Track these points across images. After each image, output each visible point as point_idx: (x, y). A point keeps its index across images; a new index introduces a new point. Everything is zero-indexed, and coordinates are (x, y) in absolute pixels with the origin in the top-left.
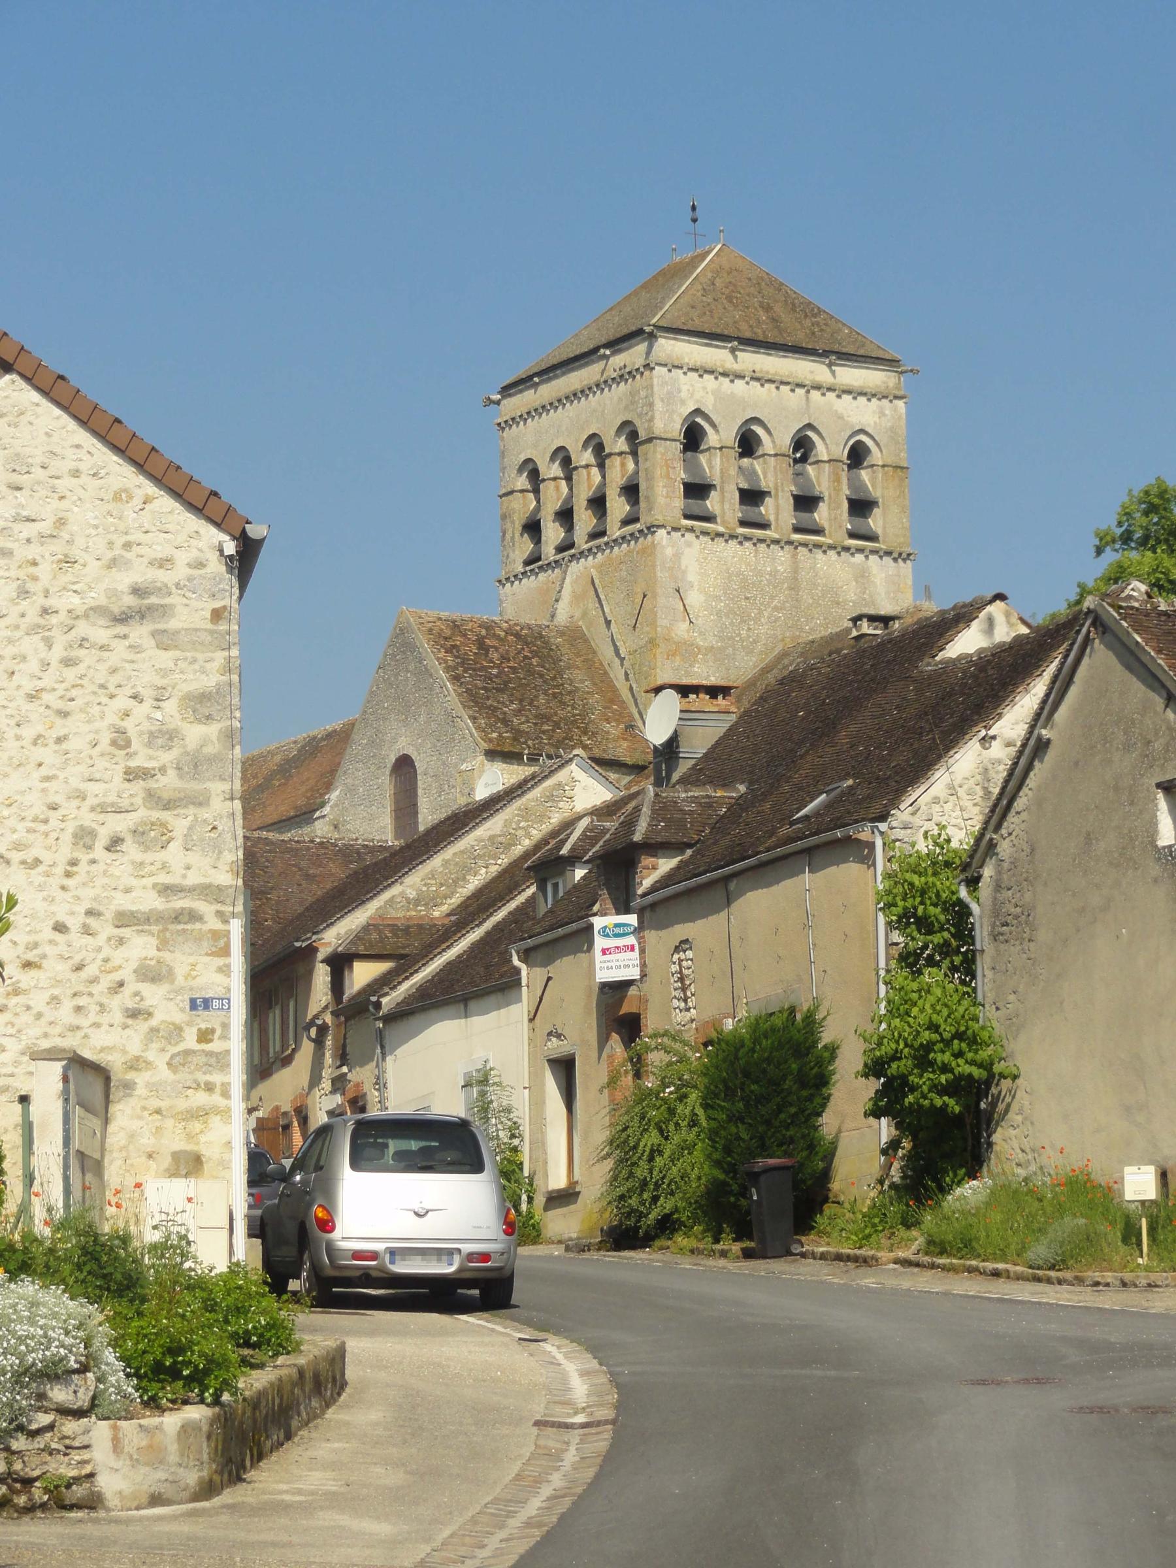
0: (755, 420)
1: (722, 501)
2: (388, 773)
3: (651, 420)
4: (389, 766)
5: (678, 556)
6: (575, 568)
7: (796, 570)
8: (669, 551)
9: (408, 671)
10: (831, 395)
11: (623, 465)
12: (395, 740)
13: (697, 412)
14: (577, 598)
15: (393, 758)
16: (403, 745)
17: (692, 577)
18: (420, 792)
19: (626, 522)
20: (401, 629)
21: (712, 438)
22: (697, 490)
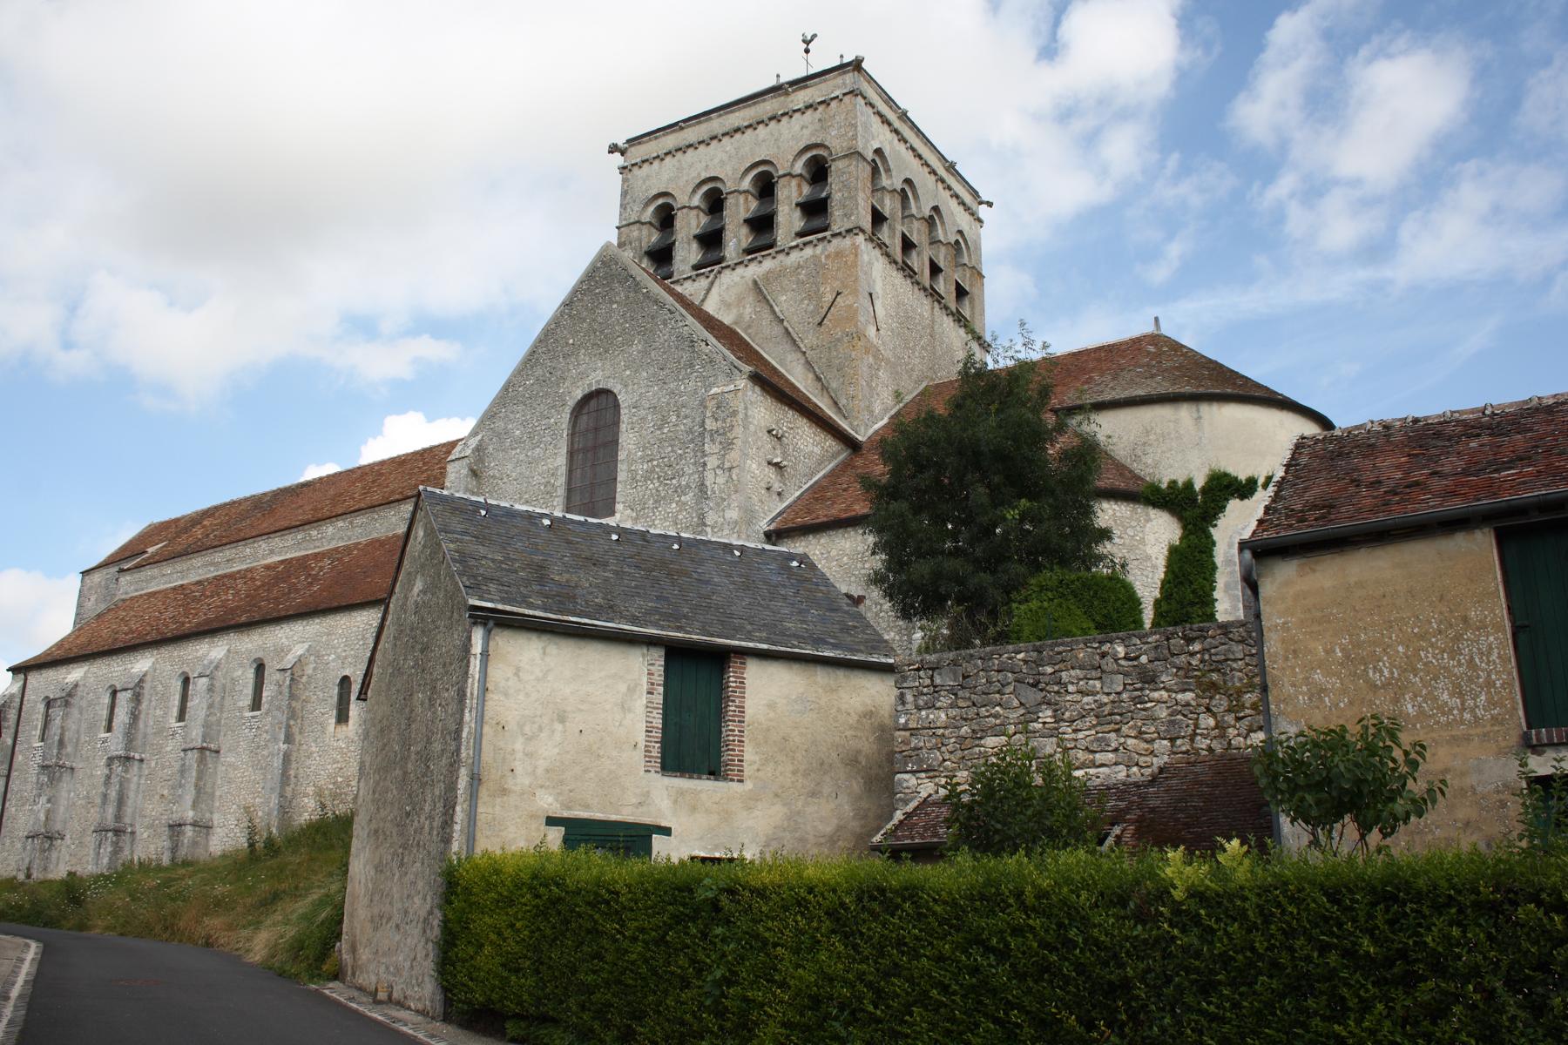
0: (908, 181)
1: (892, 236)
2: (568, 410)
3: (855, 137)
4: (571, 403)
5: (870, 263)
6: (728, 278)
7: (933, 321)
8: (866, 257)
9: (612, 302)
10: (948, 193)
11: (799, 186)
12: (582, 376)
13: (878, 152)
14: (727, 305)
15: (579, 394)
16: (598, 377)
17: (878, 289)
18: (623, 427)
19: (801, 234)
20: (603, 262)
21: (885, 181)
22: (878, 218)
